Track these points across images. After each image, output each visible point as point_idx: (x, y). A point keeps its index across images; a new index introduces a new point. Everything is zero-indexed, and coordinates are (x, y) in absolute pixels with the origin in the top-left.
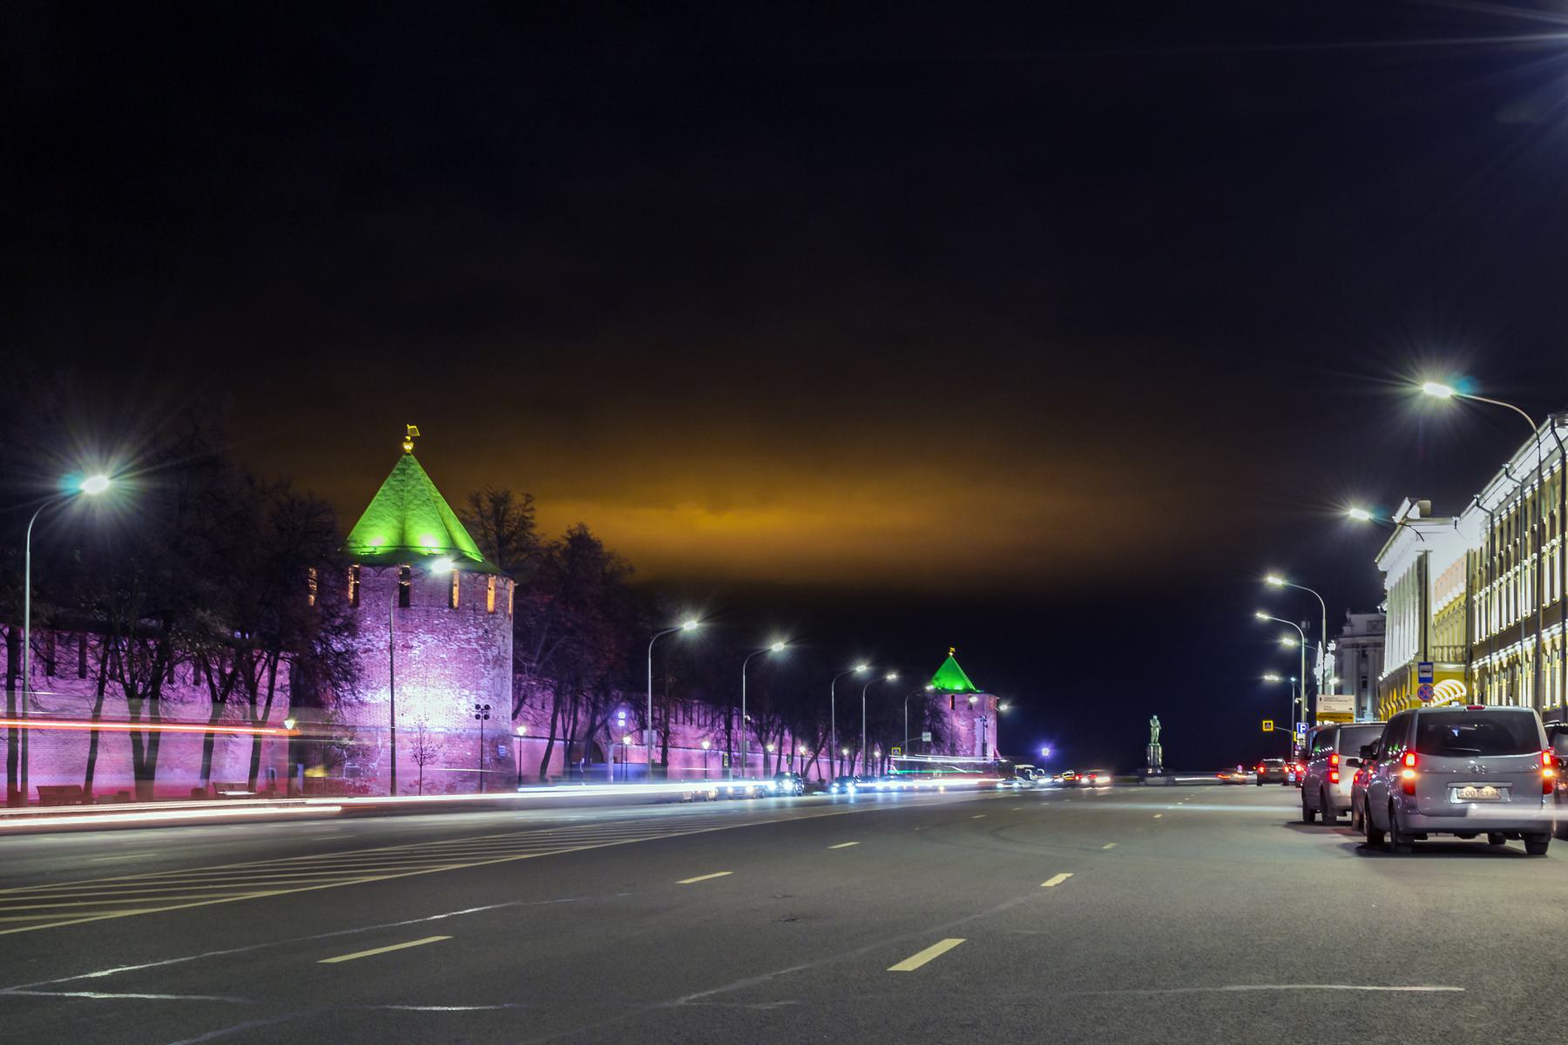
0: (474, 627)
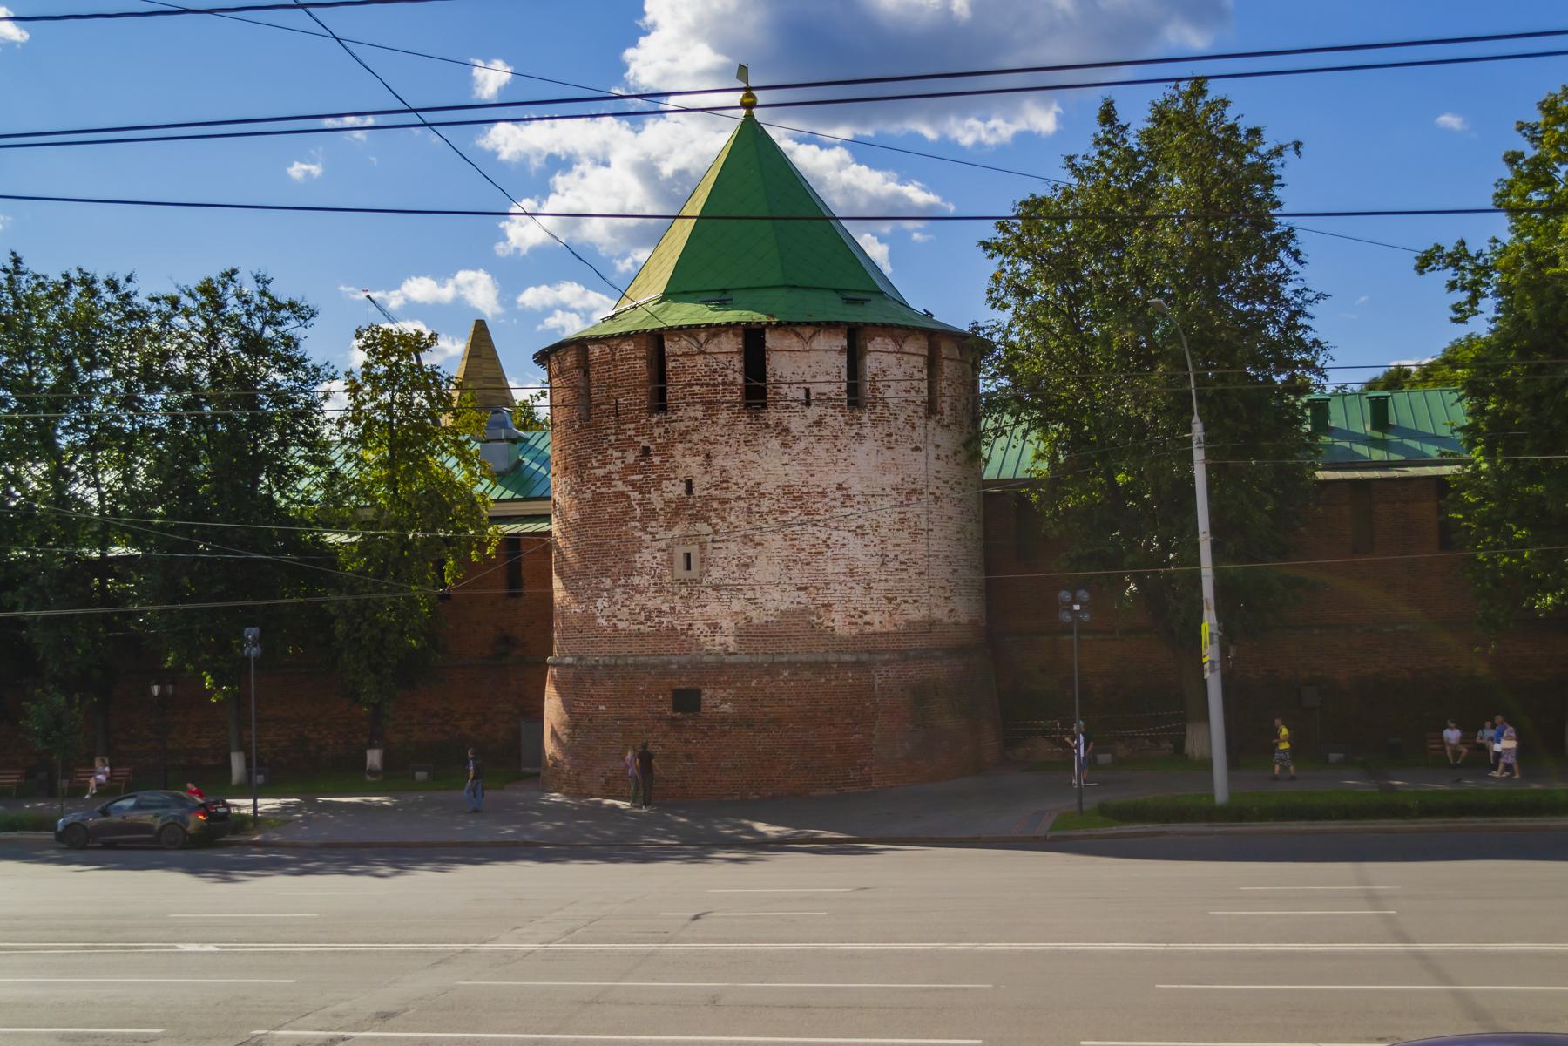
0: (617, 449)
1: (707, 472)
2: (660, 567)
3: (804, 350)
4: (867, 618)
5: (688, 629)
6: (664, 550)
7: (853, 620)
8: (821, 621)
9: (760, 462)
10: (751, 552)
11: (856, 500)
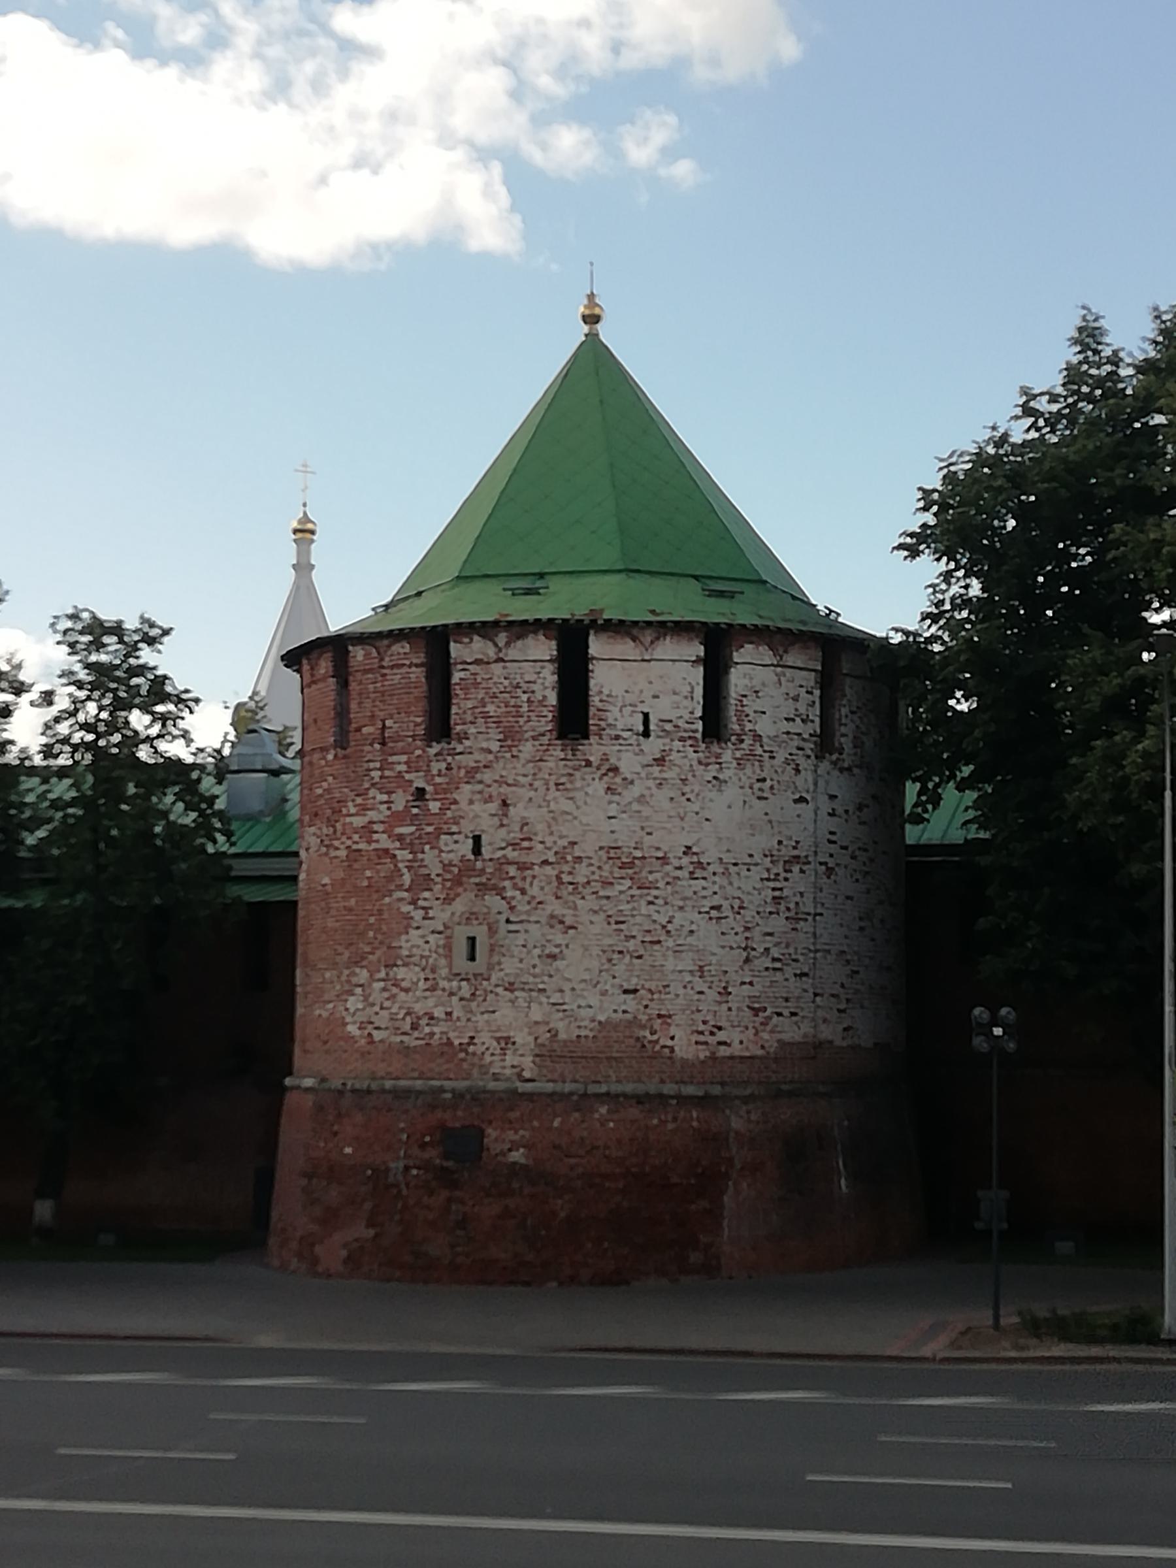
1: (502, 825)
2: (434, 955)
3: (643, 660)
4: (721, 1036)
5: (469, 1044)
6: (440, 933)
7: (702, 1038)
8: (655, 1037)
9: (576, 813)
10: (559, 939)
11: (711, 869)
